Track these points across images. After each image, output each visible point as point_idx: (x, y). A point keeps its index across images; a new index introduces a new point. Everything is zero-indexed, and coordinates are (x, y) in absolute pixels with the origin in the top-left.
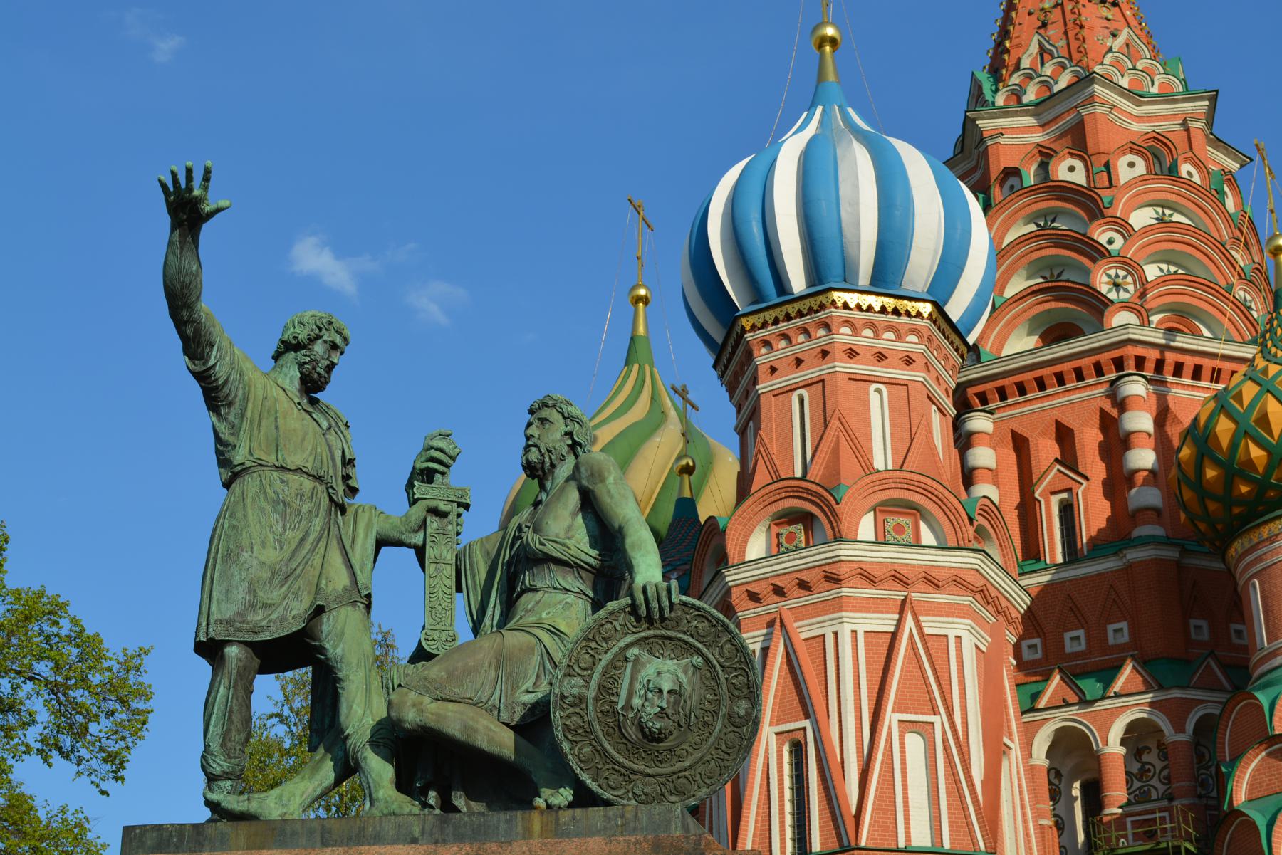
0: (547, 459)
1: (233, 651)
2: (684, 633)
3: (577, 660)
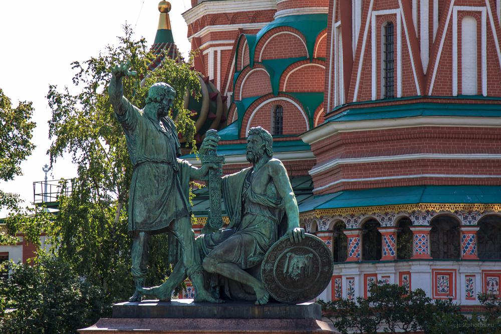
0: (256, 157)
1: (142, 234)
2: (306, 246)
3: (270, 258)
